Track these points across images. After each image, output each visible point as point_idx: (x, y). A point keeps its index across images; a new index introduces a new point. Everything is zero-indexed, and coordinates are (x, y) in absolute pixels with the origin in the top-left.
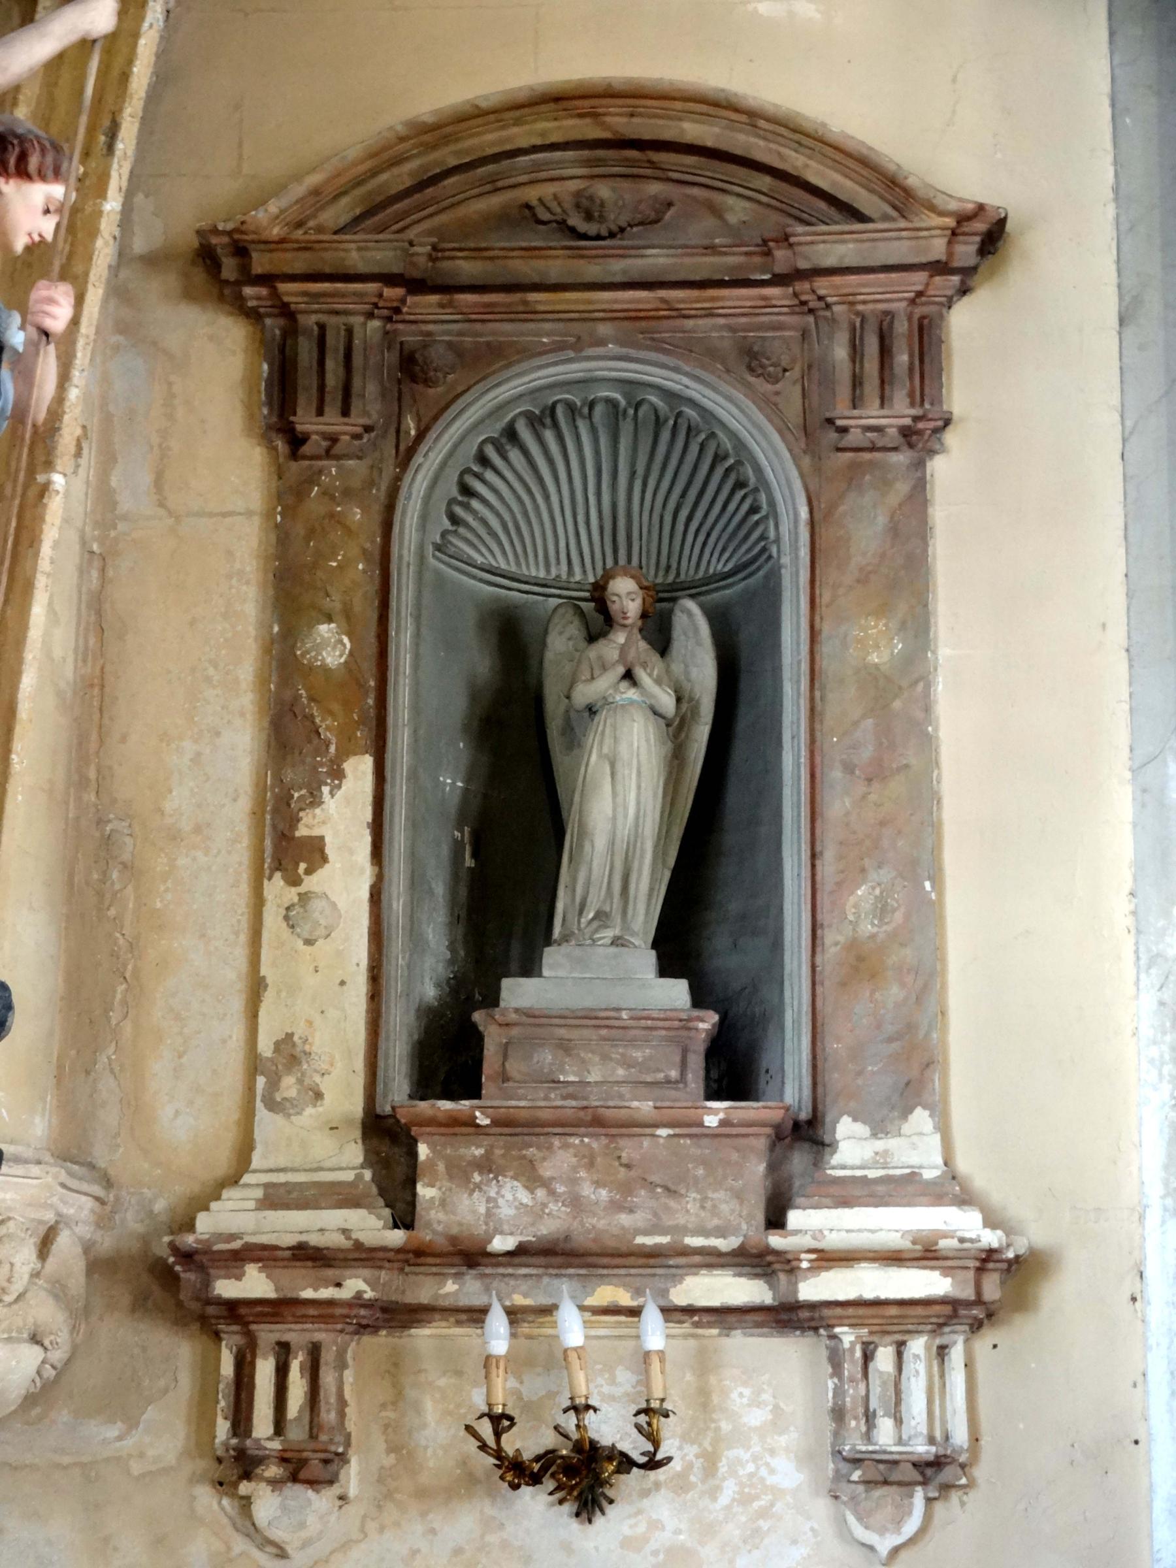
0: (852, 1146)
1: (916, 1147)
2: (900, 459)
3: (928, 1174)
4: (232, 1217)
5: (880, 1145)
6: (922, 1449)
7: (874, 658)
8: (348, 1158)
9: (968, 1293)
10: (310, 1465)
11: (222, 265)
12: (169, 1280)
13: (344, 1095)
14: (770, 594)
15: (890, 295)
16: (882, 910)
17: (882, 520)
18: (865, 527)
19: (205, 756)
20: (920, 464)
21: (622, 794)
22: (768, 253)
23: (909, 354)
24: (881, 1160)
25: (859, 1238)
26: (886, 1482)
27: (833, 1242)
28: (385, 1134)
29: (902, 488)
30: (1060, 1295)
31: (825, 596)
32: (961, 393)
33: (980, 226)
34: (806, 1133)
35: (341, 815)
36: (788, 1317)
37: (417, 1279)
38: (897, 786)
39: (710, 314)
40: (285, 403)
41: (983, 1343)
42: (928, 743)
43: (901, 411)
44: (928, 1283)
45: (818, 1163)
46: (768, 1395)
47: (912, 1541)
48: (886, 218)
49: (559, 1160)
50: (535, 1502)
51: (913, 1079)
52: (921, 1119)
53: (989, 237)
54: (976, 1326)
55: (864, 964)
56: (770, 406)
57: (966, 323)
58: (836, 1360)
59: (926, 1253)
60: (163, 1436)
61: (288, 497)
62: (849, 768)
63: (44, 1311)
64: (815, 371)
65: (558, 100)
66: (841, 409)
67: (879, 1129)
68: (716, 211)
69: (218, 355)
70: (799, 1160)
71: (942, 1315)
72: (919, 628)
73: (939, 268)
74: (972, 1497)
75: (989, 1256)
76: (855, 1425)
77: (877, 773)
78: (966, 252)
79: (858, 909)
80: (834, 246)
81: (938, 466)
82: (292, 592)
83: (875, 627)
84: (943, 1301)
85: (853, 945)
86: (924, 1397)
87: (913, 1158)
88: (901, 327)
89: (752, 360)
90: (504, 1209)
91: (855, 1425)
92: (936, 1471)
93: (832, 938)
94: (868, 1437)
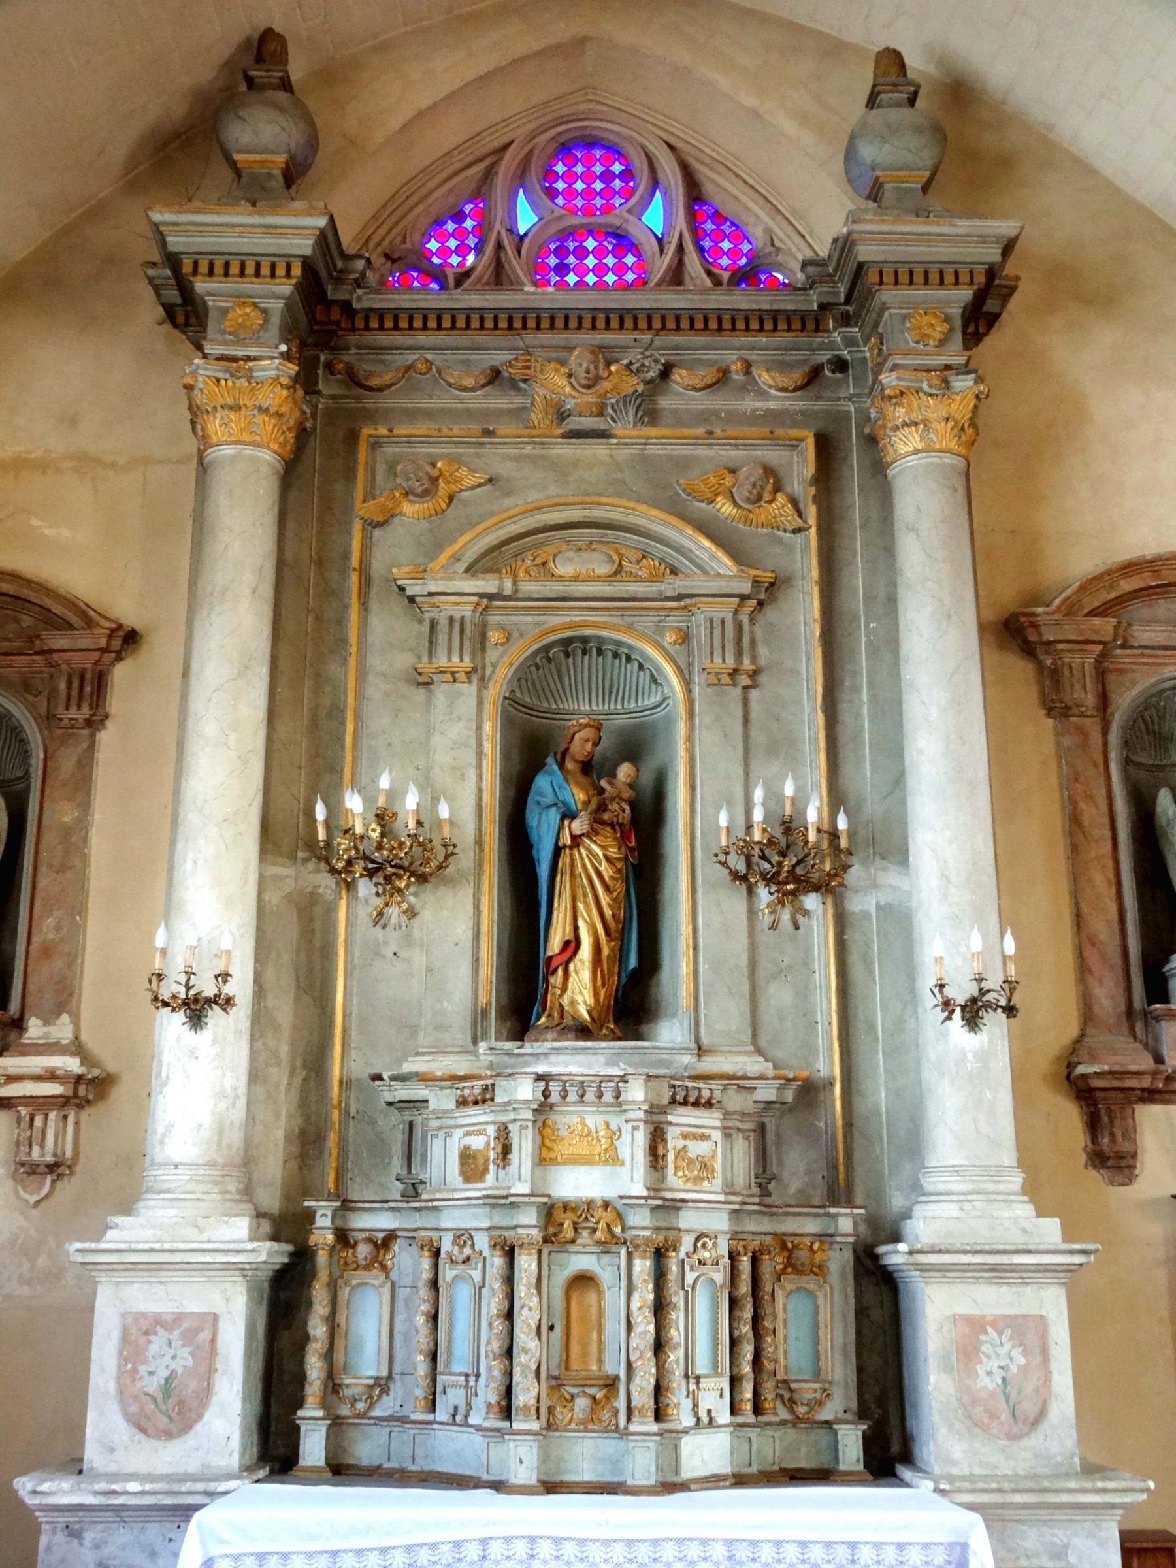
0: (35, 1029)
1: (63, 1030)
2: (85, 732)
3: (64, 1042)
5: (46, 1029)
6: (49, 1159)
7: (66, 819)
9: (70, 1093)
14: (27, 790)
15: (86, 661)
16: (58, 928)
17: (74, 758)
18: (67, 762)
20: (93, 735)
22: (32, 642)
23: (93, 688)
24: (46, 1035)
26: (34, 1173)
27: (12, 1071)
29: (84, 745)
30: (118, 1093)
31: (47, 792)
32: (116, 702)
33: (121, 633)
38: (69, 875)
39: (10, 666)
41: (84, 1115)
42: (85, 858)
43: (86, 712)
44: (54, 1089)
45: (20, 1037)
47: (47, 1196)
48: (83, 629)
51: (64, 1000)
52: (65, 1018)
53: (131, 638)
54: (80, 1107)
55: (47, 952)
56: (32, 708)
57: (121, 673)
58: (19, 1120)
59: (51, 1076)
62: (50, 866)
64: (53, 695)
66: (60, 712)
67: (47, 1022)
68: (17, 621)
70: (13, 1035)
71: (63, 1102)
72: (86, 806)
73: (104, 651)
74: (73, 1179)
75: (79, 1079)
76: (24, 1149)
77: (61, 870)
78: (116, 644)
79: (47, 928)
80: (59, 641)
81: (105, 738)
83: (66, 806)
84: (61, 1096)
85: (44, 942)
86: (54, 1136)
87: (60, 1035)
88: (89, 675)
89: (25, 687)
91: (24, 1149)
92: (52, 1168)
93: (36, 939)
94: (29, 1154)
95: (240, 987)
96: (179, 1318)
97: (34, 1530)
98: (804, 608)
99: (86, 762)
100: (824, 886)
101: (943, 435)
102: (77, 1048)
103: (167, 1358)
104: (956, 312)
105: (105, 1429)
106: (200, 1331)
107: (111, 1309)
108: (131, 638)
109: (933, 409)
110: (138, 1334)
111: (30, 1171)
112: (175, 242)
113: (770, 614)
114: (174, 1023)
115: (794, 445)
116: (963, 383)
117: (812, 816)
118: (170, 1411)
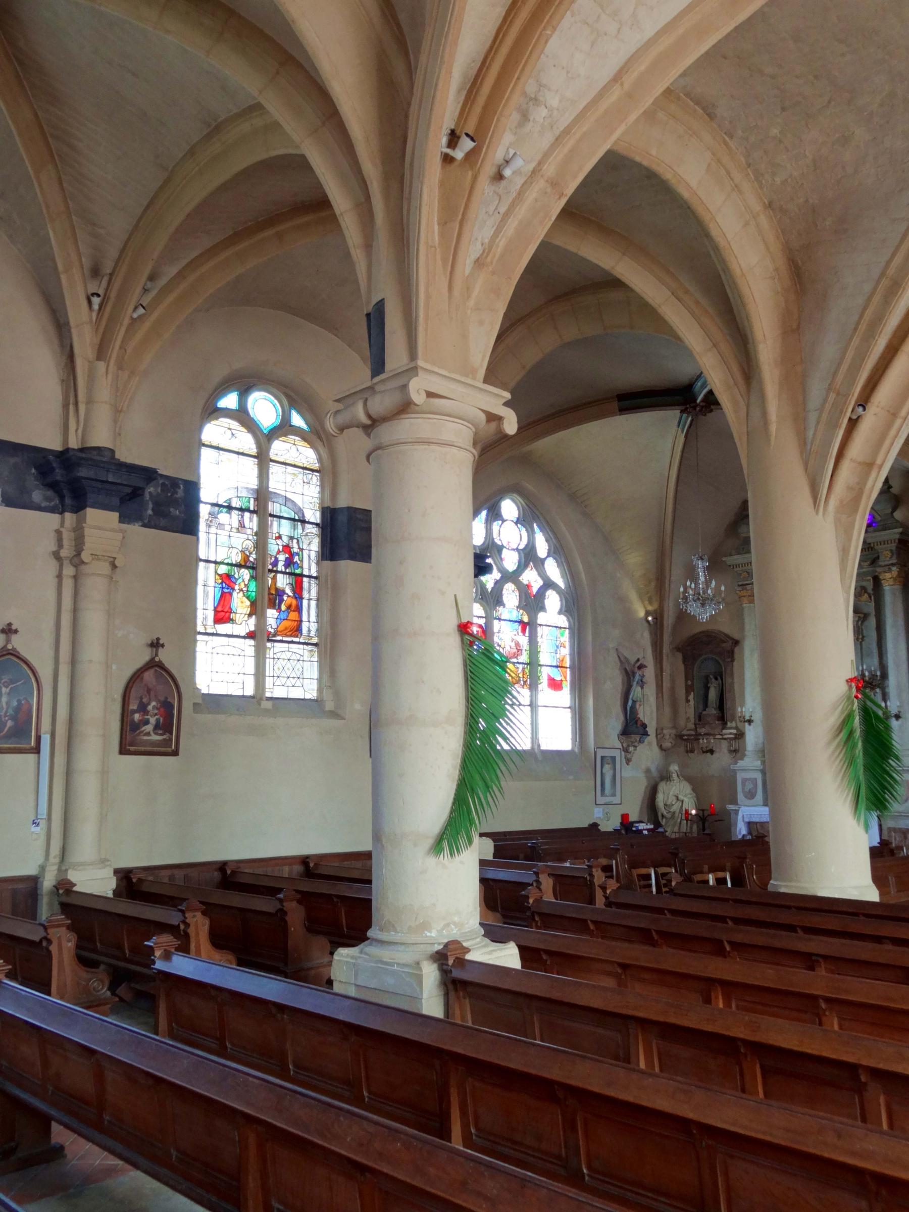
0: (729, 724)
1: (734, 724)
4: (684, 732)
8: (693, 726)
10: (692, 751)
11: (678, 649)
12: (680, 737)
13: (692, 720)
19: (681, 691)
21: (713, 694)
23: (731, 654)
25: (729, 732)
28: (695, 724)
32: (736, 656)
34: (726, 723)
35: (691, 697)
36: (725, 739)
37: (697, 737)
40: (685, 660)
46: (725, 744)
49: (707, 727)
50: (709, 754)
51: (733, 719)
57: (736, 650)
59: (731, 734)
60: (682, 749)
61: (686, 669)
63: (671, 740)
65: (703, 632)
69: (680, 656)
71: (735, 739)
72: (733, 679)
80: (724, 645)
81: (735, 663)
82: (686, 680)
86: (735, 745)
90: (703, 731)
92: (735, 751)
95: (758, 716)
96: (750, 779)
97: (730, 814)
98: (872, 622)
99: (732, 670)
100: (878, 686)
101: (891, 582)
102: (737, 728)
103: (749, 786)
104: (894, 548)
105: (740, 797)
106: (754, 781)
107: (740, 777)
108: (736, 643)
109: (888, 575)
110: (744, 781)
111: (731, 751)
112: (729, 563)
113: (866, 623)
114: (746, 724)
115: (869, 580)
116: (894, 568)
117: (867, 674)
118: (751, 795)
